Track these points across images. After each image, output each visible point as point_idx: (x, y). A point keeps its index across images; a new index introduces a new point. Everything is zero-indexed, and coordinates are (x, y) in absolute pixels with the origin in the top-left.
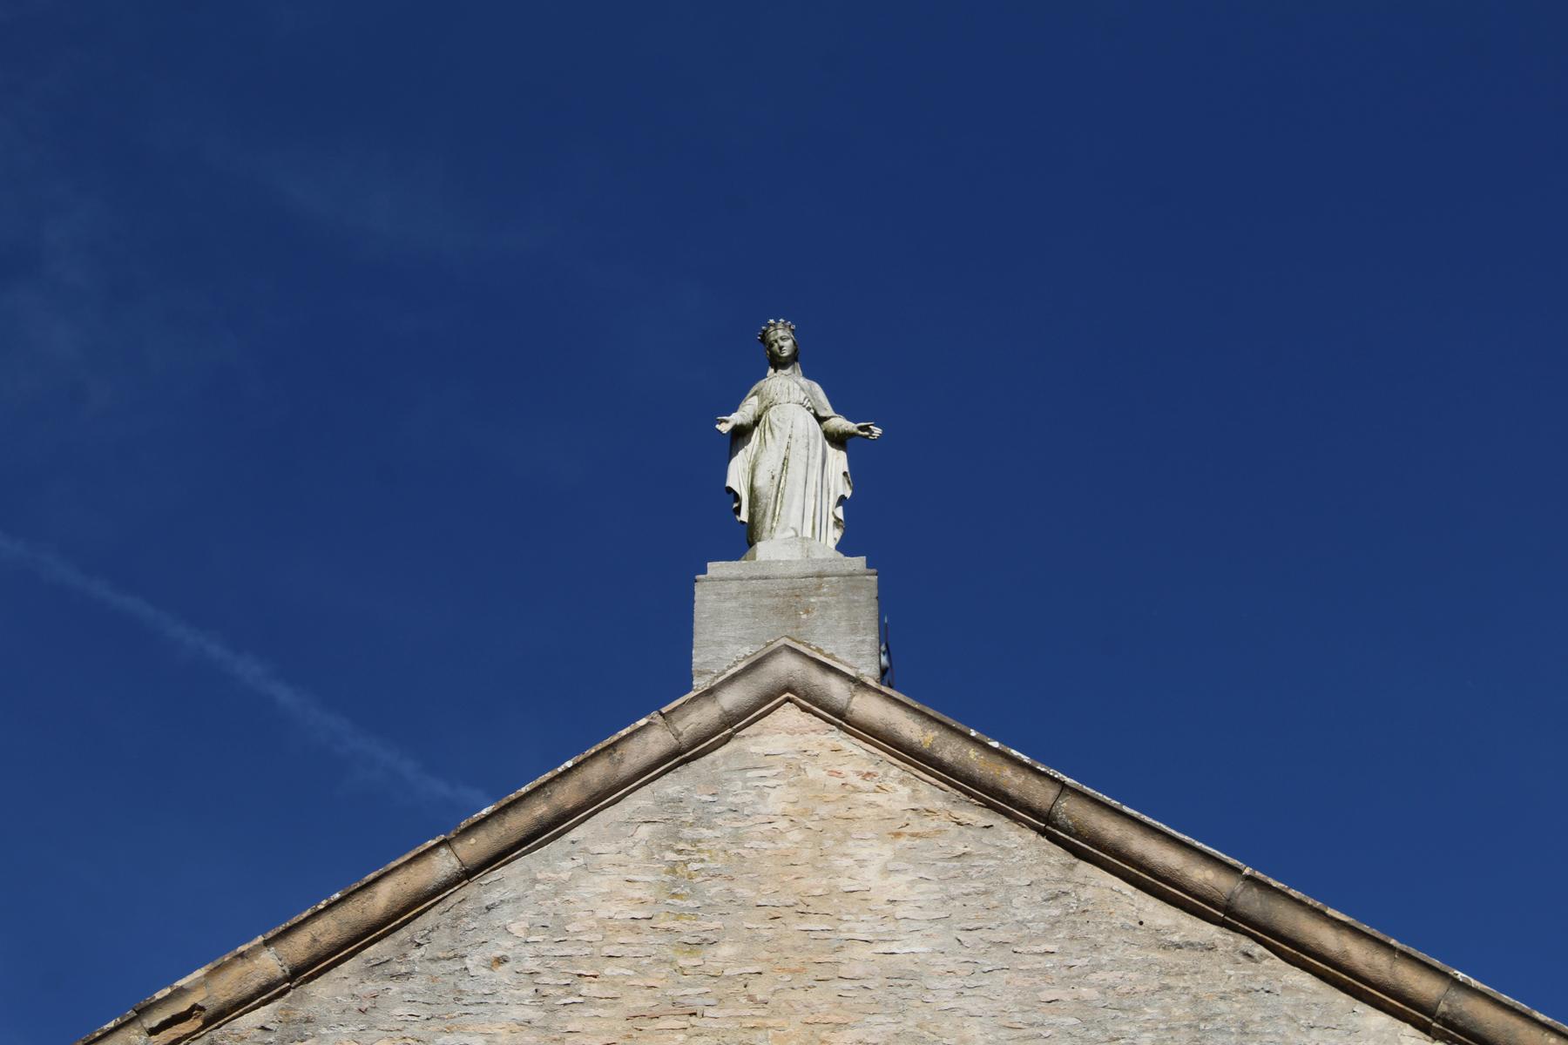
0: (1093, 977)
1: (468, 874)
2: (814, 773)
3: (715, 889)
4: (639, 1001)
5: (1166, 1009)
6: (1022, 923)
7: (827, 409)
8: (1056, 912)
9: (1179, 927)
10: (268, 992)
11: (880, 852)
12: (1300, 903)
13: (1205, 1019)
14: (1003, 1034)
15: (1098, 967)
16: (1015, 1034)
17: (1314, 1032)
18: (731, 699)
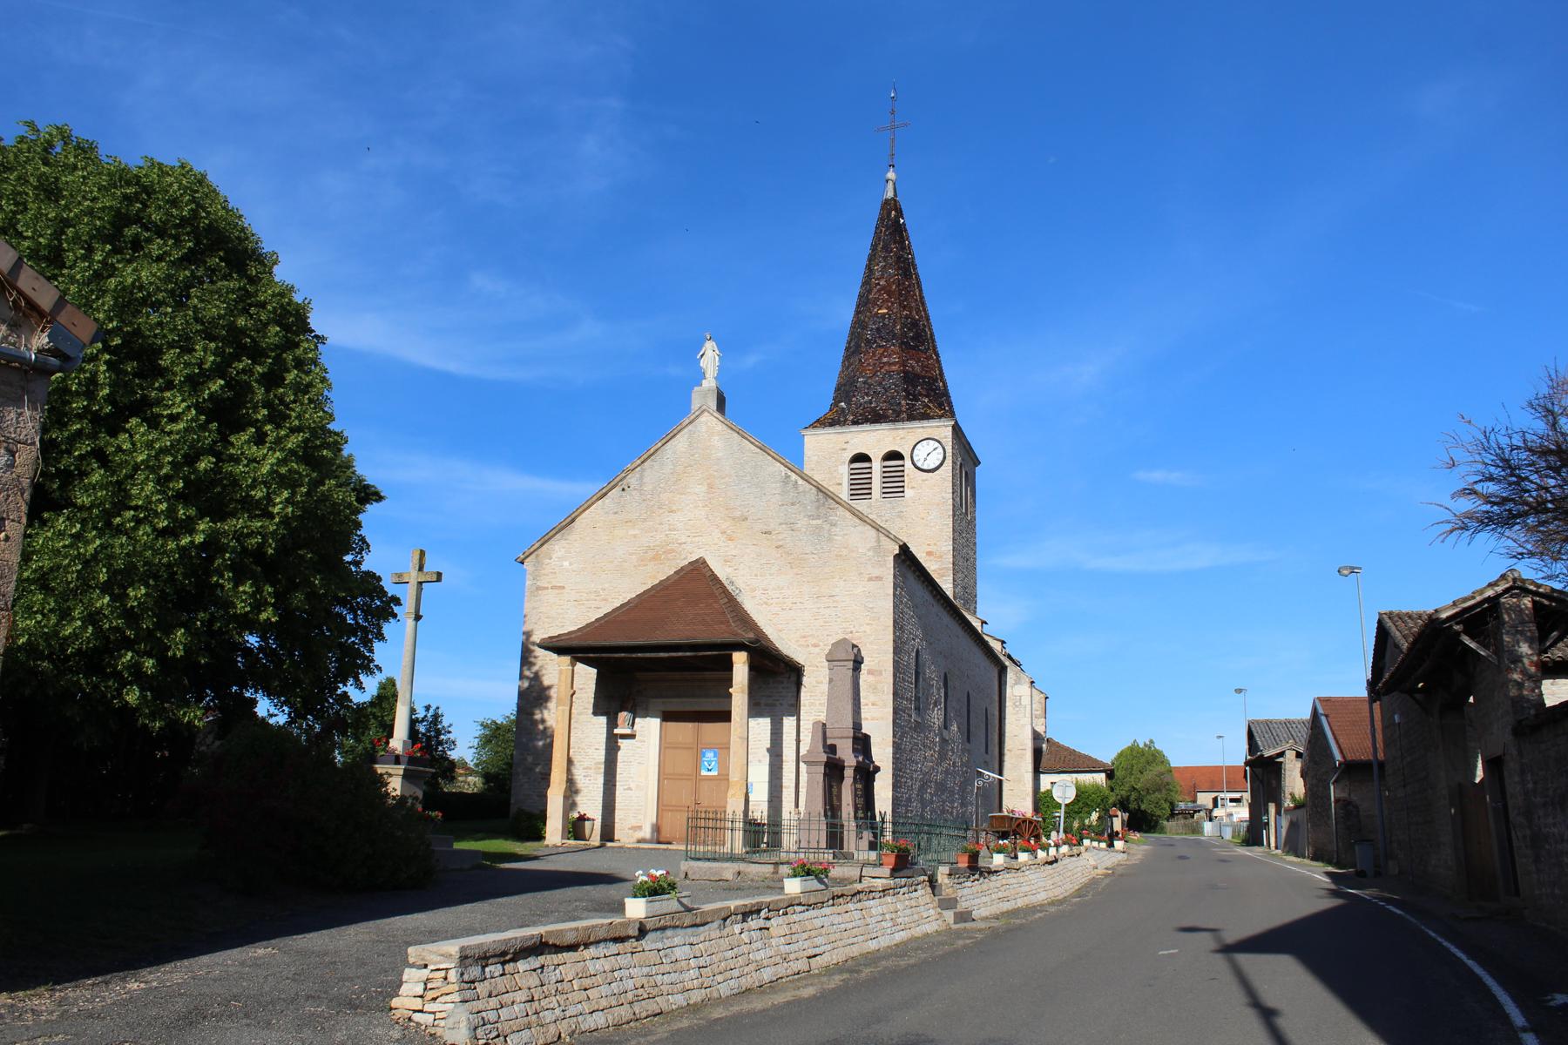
1: (663, 445)
2: (709, 424)
3: (695, 445)
4: (686, 465)
7: (716, 349)
10: (639, 465)
11: (717, 438)
18: (697, 413)
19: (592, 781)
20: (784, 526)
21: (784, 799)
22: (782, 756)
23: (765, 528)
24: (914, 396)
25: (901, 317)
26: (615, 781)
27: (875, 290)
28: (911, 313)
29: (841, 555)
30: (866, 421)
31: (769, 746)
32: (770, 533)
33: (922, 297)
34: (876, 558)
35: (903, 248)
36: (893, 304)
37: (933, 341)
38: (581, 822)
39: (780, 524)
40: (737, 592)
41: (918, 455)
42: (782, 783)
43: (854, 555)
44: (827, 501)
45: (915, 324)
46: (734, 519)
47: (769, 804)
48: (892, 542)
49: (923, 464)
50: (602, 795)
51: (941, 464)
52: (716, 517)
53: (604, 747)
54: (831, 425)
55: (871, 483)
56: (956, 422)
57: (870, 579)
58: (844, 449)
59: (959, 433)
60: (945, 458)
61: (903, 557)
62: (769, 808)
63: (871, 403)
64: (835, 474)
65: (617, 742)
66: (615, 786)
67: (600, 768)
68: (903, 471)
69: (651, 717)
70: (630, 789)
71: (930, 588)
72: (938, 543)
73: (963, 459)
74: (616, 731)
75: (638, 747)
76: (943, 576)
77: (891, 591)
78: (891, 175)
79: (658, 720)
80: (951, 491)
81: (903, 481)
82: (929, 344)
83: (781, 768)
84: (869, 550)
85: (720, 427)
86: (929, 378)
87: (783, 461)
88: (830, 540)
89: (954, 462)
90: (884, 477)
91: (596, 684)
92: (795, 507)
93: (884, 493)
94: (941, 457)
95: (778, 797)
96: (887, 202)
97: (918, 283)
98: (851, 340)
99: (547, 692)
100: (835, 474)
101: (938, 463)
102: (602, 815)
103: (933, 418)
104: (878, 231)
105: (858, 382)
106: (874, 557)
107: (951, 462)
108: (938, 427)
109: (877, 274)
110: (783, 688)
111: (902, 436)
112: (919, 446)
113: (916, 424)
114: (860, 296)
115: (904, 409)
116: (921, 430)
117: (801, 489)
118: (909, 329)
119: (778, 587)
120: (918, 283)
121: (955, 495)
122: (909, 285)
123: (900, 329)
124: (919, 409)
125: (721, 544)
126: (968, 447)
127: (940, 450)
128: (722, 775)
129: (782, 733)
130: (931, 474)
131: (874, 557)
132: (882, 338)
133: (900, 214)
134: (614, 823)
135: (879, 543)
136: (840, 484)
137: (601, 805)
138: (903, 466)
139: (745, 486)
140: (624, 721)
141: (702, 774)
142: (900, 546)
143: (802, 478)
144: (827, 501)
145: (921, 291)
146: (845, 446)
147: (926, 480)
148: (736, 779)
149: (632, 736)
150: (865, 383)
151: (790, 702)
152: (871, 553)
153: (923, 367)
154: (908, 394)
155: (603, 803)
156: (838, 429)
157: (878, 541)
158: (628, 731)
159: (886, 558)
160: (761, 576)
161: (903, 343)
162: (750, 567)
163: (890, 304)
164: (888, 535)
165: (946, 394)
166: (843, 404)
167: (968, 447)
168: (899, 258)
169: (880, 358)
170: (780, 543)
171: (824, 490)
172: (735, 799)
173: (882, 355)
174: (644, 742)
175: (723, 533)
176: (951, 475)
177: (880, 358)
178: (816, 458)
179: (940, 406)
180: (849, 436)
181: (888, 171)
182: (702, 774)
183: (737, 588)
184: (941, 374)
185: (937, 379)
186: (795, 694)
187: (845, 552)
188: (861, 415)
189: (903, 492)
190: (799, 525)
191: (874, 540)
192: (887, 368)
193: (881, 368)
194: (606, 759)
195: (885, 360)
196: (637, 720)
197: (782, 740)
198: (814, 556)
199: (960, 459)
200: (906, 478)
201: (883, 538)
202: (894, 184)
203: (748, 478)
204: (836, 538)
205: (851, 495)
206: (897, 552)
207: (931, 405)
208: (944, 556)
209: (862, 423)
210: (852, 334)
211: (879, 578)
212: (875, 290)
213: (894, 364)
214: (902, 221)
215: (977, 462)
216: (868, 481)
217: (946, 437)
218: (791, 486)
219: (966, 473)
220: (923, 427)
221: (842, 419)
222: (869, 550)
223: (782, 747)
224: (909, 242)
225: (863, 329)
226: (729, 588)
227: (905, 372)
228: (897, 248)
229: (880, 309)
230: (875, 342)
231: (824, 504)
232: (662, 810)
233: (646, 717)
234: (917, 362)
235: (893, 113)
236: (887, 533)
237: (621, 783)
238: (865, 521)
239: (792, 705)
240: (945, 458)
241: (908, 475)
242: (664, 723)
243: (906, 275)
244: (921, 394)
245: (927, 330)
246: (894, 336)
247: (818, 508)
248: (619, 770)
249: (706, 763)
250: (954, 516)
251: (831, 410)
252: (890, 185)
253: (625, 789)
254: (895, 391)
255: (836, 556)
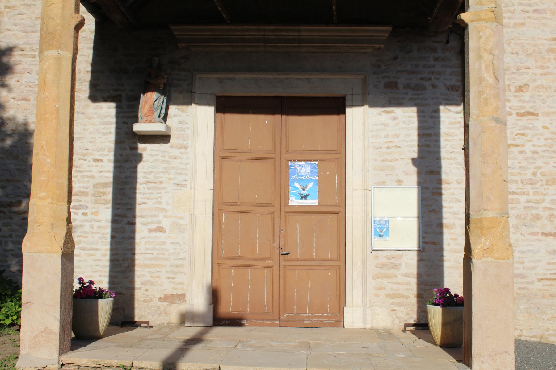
19: (89, 216)
21: (445, 247)
22: (439, 173)
26: (134, 217)
31: (415, 155)
38: (89, 302)
42: (441, 218)
47: (418, 255)
50: (109, 239)
53: (111, 156)
62: (420, 260)
65: (136, 148)
66: (134, 224)
67: (104, 194)
69: (199, 104)
70: (160, 229)
74: (138, 127)
75: (175, 158)
79: (211, 110)
83: (439, 193)
91: (95, 49)
95: (434, 243)
99: (5, 59)
102: (111, 277)
110: (436, 59)
128: (327, 205)
129: (437, 135)
134: (133, 289)
137: (108, 257)
140: (151, 110)
141: (290, 204)
148: (491, 214)
149: (163, 138)
151: (448, 83)
155: (112, 255)
158: (157, 127)
172: (490, 259)
174: (186, 147)
182: (290, 204)
186: (459, 70)
194: (115, 178)
196: (173, 109)
197: (439, 147)
223: (439, 159)
232: (219, 265)
233: (189, 103)
237: (145, 220)
239: (452, 88)
242: (220, 115)
248: (139, 198)
249: (297, 185)
253: (150, 231)
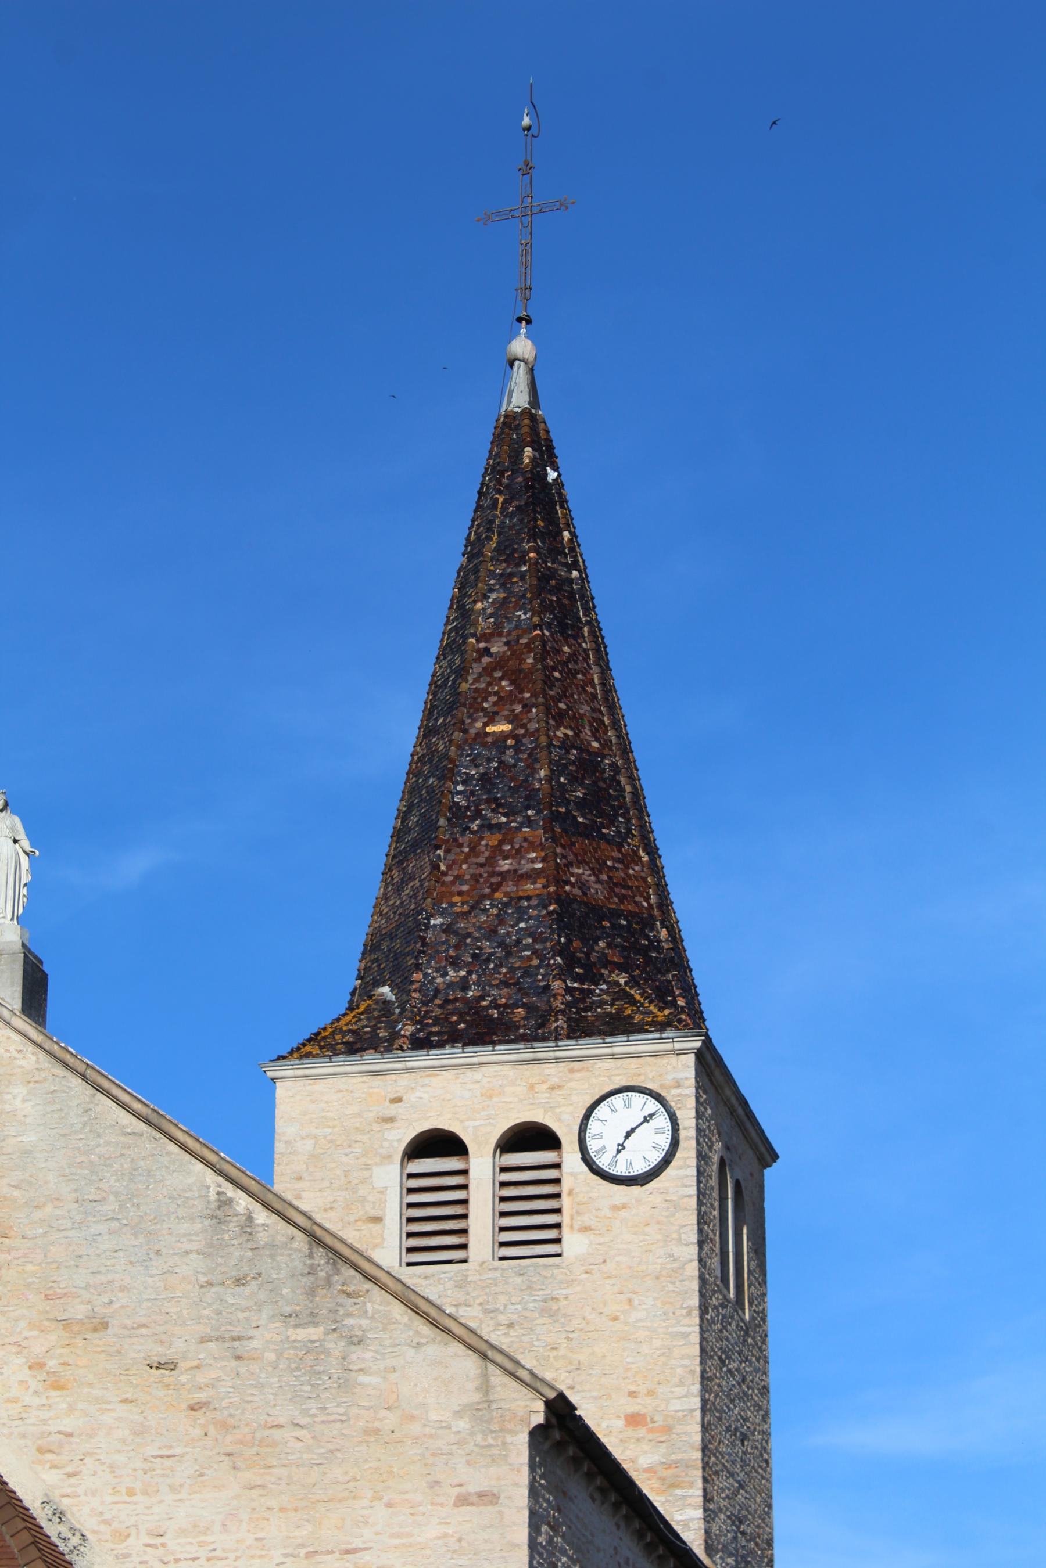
0: (97, 1150)
5: (122, 1165)
6: (72, 1125)
7: (22, 836)
8: (85, 1119)
9: (131, 1124)
11: (21, 1091)
12: (170, 1121)
13: (135, 1170)
14: (61, 1179)
15: (99, 1145)
16: (65, 1178)
17: (175, 1173)
20: (212, 1345)
23: (158, 1352)
24: (588, 966)
25: (550, 745)
27: (477, 669)
28: (577, 735)
29: (377, 1431)
30: (452, 1038)
32: (171, 1366)
33: (609, 690)
34: (479, 1438)
35: (555, 550)
36: (527, 707)
37: (642, 811)
39: (203, 1340)
40: (75, 1541)
41: (599, 1136)
43: (416, 1428)
44: (338, 1272)
45: (589, 764)
46: (66, 1324)
48: (525, 1390)
49: (614, 1161)
51: (666, 1162)
52: (16, 1320)
54: (352, 1049)
55: (465, 1216)
56: (708, 1043)
57: (463, 1501)
58: (391, 1120)
59: (717, 1073)
60: (675, 1143)
61: (557, 1435)
63: (465, 987)
64: (362, 1192)
68: (557, 1181)
71: (637, 1524)
72: (660, 1390)
73: (727, 1148)
76: (674, 1486)
77: (521, 1534)
78: (522, 346)
80: (694, 1237)
81: (558, 1211)
82: (628, 820)
84: (458, 1414)
85: (31, 1059)
86: (630, 916)
87: (212, 1157)
88: (345, 1385)
89: (702, 1157)
90: (503, 1199)
92: (247, 1290)
93: (503, 1244)
94: (665, 1141)
96: (510, 417)
97: (597, 651)
98: (410, 807)
100: (362, 1192)
101: (655, 1157)
103: (641, 1029)
104: (486, 503)
105: (427, 926)
106: (472, 1434)
107: (693, 1154)
108: (654, 1055)
109: (484, 624)
111: (555, 1080)
112: (602, 1111)
113: (593, 1047)
114: (436, 687)
115: (558, 1004)
116: (608, 1064)
117: (263, 1238)
118: (573, 779)
119: (195, 1526)
120: (597, 651)
121: (706, 1248)
122: (573, 657)
123: (549, 779)
124: (601, 1004)
125: (29, 1399)
126: (740, 1111)
127: (662, 1121)
130: (636, 1190)
131: (472, 1434)
132: (498, 805)
133: (547, 454)
135: (487, 1392)
136: (377, 1220)
138: (557, 1166)
139: (102, 1228)
142: (548, 1404)
143: (266, 1205)
144: (338, 1272)
145: (605, 670)
146: (392, 1110)
147: (624, 1206)
150: (447, 929)
152: (463, 1424)
153: (612, 885)
154: (571, 961)
156: (371, 1061)
157: (485, 1387)
159: (509, 1439)
160: (145, 1493)
161: (555, 817)
162: (112, 1468)
163: (518, 709)
164: (513, 1370)
165: (678, 961)
166: (385, 990)
167: (740, 1111)
168: (544, 579)
169: (491, 861)
170: (202, 1396)
171: (329, 1240)
173: (497, 849)
175: (36, 1366)
176: (694, 1191)
177: (491, 861)
178: (309, 1144)
179: (662, 995)
180: (400, 1083)
181: (513, 335)
183: (73, 1530)
184: (665, 904)
185: (652, 917)
187: (390, 1420)
188: (437, 1021)
189: (558, 1241)
190: (255, 1344)
191: (471, 1386)
192: (510, 887)
193: (495, 888)
195: (505, 865)
198: (300, 1433)
199: (718, 1146)
200: (566, 1202)
201: (498, 1379)
202: (531, 371)
203: (111, 1206)
204: (362, 1378)
205: (411, 1250)
206: (539, 1419)
207: (636, 994)
208: (678, 1429)
209: (441, 1045)
210: (412, 790)
211: (487, 1498)
212: (477, 669)
213: (532, 876)
214: (552, 475)
215: (767, 1155)
216: (458, 1210)
217: (678, 1085)
218: (233, 1227)
219: (737, 1185)
220: (613, 1056)
221: (383, 1034)
222: (458, 1414)
224: (573, 535)
225: (442, 778)
226: (52, 1530)
227: (564, 902)
228: (536, 550)
229: (491, 721)
230: (478, 814)
231: (328, 1282)
234: (596, 872)
235: (527, 169)
236: (509, 1365)
238: (447, 1331)
240: (675, 1143)
241: (570, 1193)
243: (563, 627)
244: (606, 963)
245: (623, 780)
246: (531, 799)
247: (311, 1293)
250: (704, 1309)
251: (351, 1009)
252: (520, 376)
254: (535, 952)
255: (367, 1432)
